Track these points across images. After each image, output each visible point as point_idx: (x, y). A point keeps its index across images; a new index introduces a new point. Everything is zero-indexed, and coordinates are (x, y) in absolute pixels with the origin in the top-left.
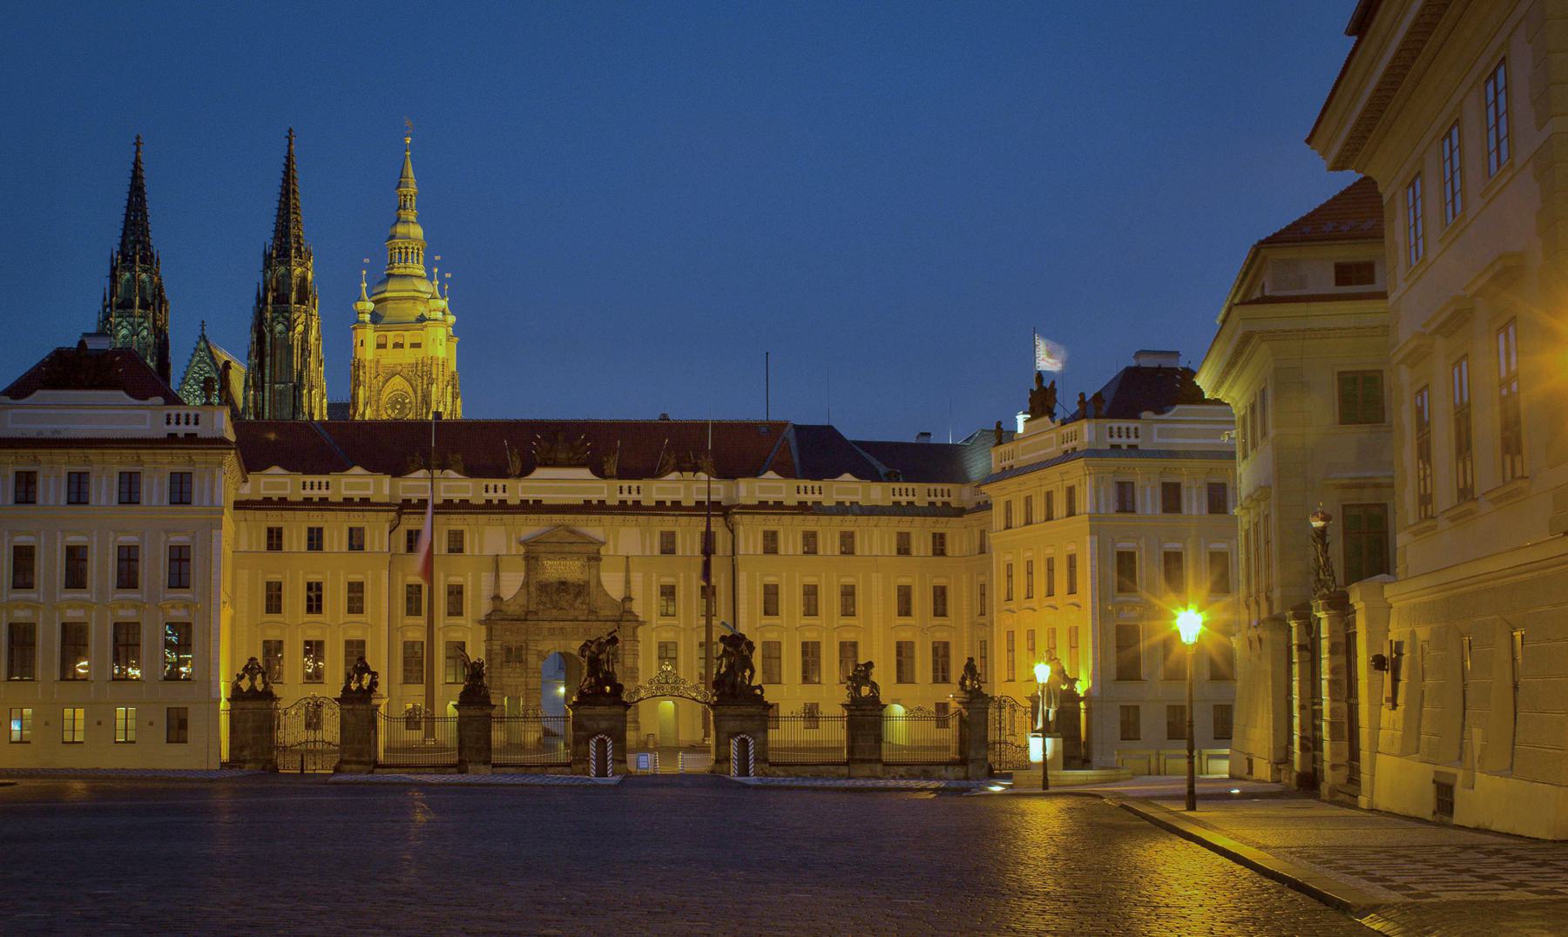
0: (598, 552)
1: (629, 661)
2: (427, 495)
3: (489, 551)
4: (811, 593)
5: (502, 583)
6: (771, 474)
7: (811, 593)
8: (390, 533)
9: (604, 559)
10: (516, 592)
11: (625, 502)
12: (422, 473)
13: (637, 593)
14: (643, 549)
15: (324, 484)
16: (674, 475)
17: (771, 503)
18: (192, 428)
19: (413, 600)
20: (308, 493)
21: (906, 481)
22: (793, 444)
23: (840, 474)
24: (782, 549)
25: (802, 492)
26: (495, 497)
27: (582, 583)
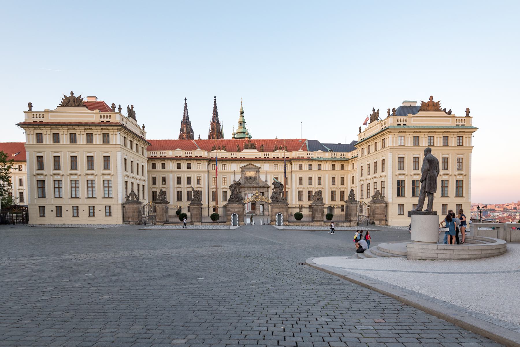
1: (266, 196)
3: (233, 170)
4: (310, 179)
6: (301, 150)
7: (310, 179)
8: (208, 165)
12: (215, 151)
13: (269, 180)
15: (190, 153)
16: (277, 151)
17: (301, 157)
20: (187, 155)
22: (307, 144)
24: (303, 169)
25: (308, 154)
26: (234, 156)
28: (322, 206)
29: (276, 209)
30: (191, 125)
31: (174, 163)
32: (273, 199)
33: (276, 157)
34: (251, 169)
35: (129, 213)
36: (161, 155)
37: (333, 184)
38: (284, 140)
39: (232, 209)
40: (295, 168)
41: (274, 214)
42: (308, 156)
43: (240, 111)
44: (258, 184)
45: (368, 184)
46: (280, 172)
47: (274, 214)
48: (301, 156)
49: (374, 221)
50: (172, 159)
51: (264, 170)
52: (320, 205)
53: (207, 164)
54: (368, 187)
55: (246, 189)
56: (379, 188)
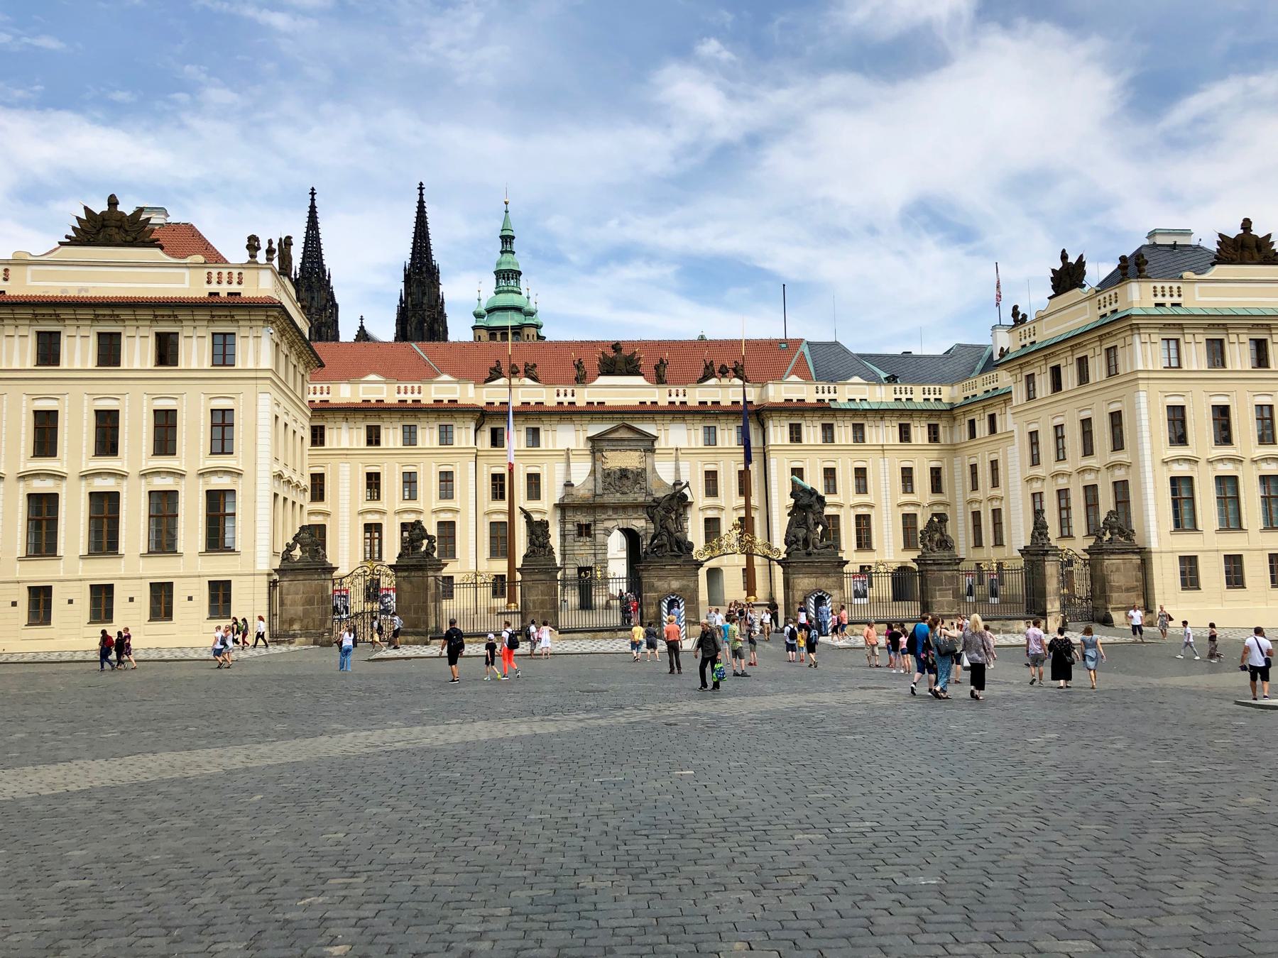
0: (653, 445)
2: (506, 400)
3: (561, 446)
6: (794, 378)
8: (476, 431)
9: (657, 451)
11: (674, 403)
12: (501, 381)
14: (689, 442)
16: (713, 381)
17: (795, 401)
18: (235, 288)
19: (499, 486)
20: (402, 396)
21: (905, 381)
23: (849, 378)
24: (805, 441)
27: (640, 470)
28: (956, 568)
29: (806, 581)
30: (329, 281)
31: (358, 425)
32: (794, 546)
33: (709, 400)
35: (290, 605)
37: (905, 491)
38: (741, 340)
39: (660, 583)
40: (775, 437)
41: (798, 596)
42: (820, 396)
43: (499, 233)
45: (1063, 494)
46: (728, 452)
47: (798, 596)
48: (795, 397)
49: (1110, 611)
50: (349, 412)
52: (948, 564)
53: (472, 426)
54: (1063, 502)
55: (610, 513)
56: (1106, 503)
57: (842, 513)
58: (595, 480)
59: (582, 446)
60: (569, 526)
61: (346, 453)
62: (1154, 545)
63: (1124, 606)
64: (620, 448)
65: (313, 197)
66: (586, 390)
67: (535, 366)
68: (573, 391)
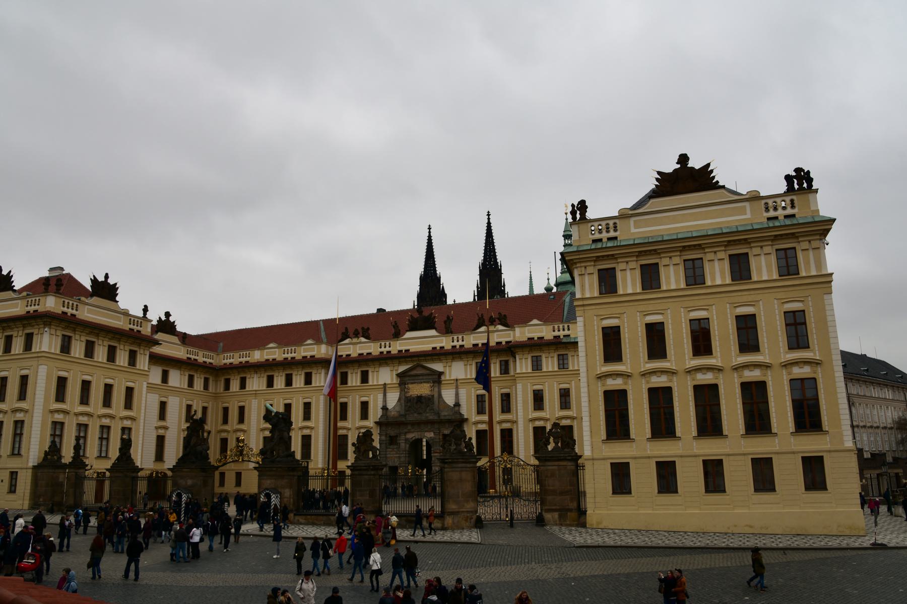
3: (381, 382)
5: (387, 399)
9: (443, 382)
10: (394, 404)
11: (455, 346)
14: (466, 375)
17: (536, 339)
20: (286, 356)
27: (430, 396)
29: (269, 482)
34: (421, 377)
36: (241, 360)
42: (556, 333)
44: (438, 414)
48: (536, 335)
49: (543, 513)
51: (452, 378)
55: (409, 427)
57: (575, 423)
58: (401, 404)
59: (395, 381)
60: (383, 438)
61: (256, 393)
62: (587, 452)
63: (558, 507)
64: (416, 381)
65: (430, 231)
66: (398, 342)
67: (368, 329)
68: (390, 343)
